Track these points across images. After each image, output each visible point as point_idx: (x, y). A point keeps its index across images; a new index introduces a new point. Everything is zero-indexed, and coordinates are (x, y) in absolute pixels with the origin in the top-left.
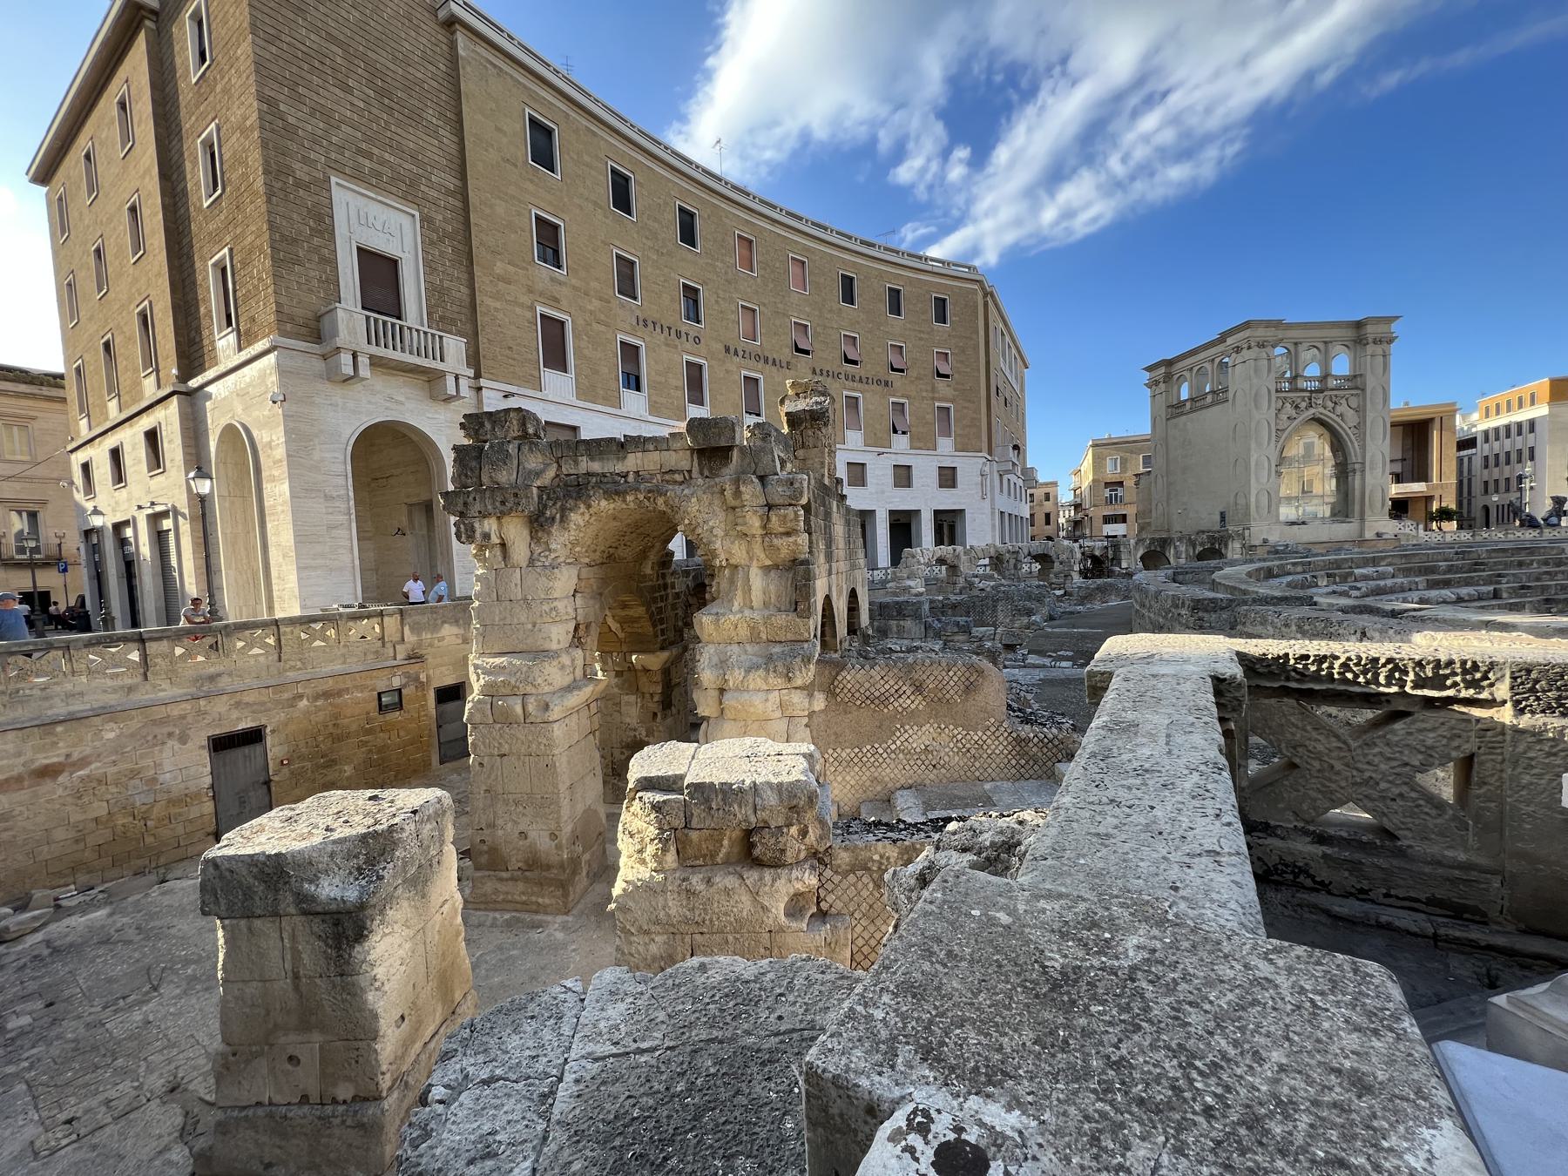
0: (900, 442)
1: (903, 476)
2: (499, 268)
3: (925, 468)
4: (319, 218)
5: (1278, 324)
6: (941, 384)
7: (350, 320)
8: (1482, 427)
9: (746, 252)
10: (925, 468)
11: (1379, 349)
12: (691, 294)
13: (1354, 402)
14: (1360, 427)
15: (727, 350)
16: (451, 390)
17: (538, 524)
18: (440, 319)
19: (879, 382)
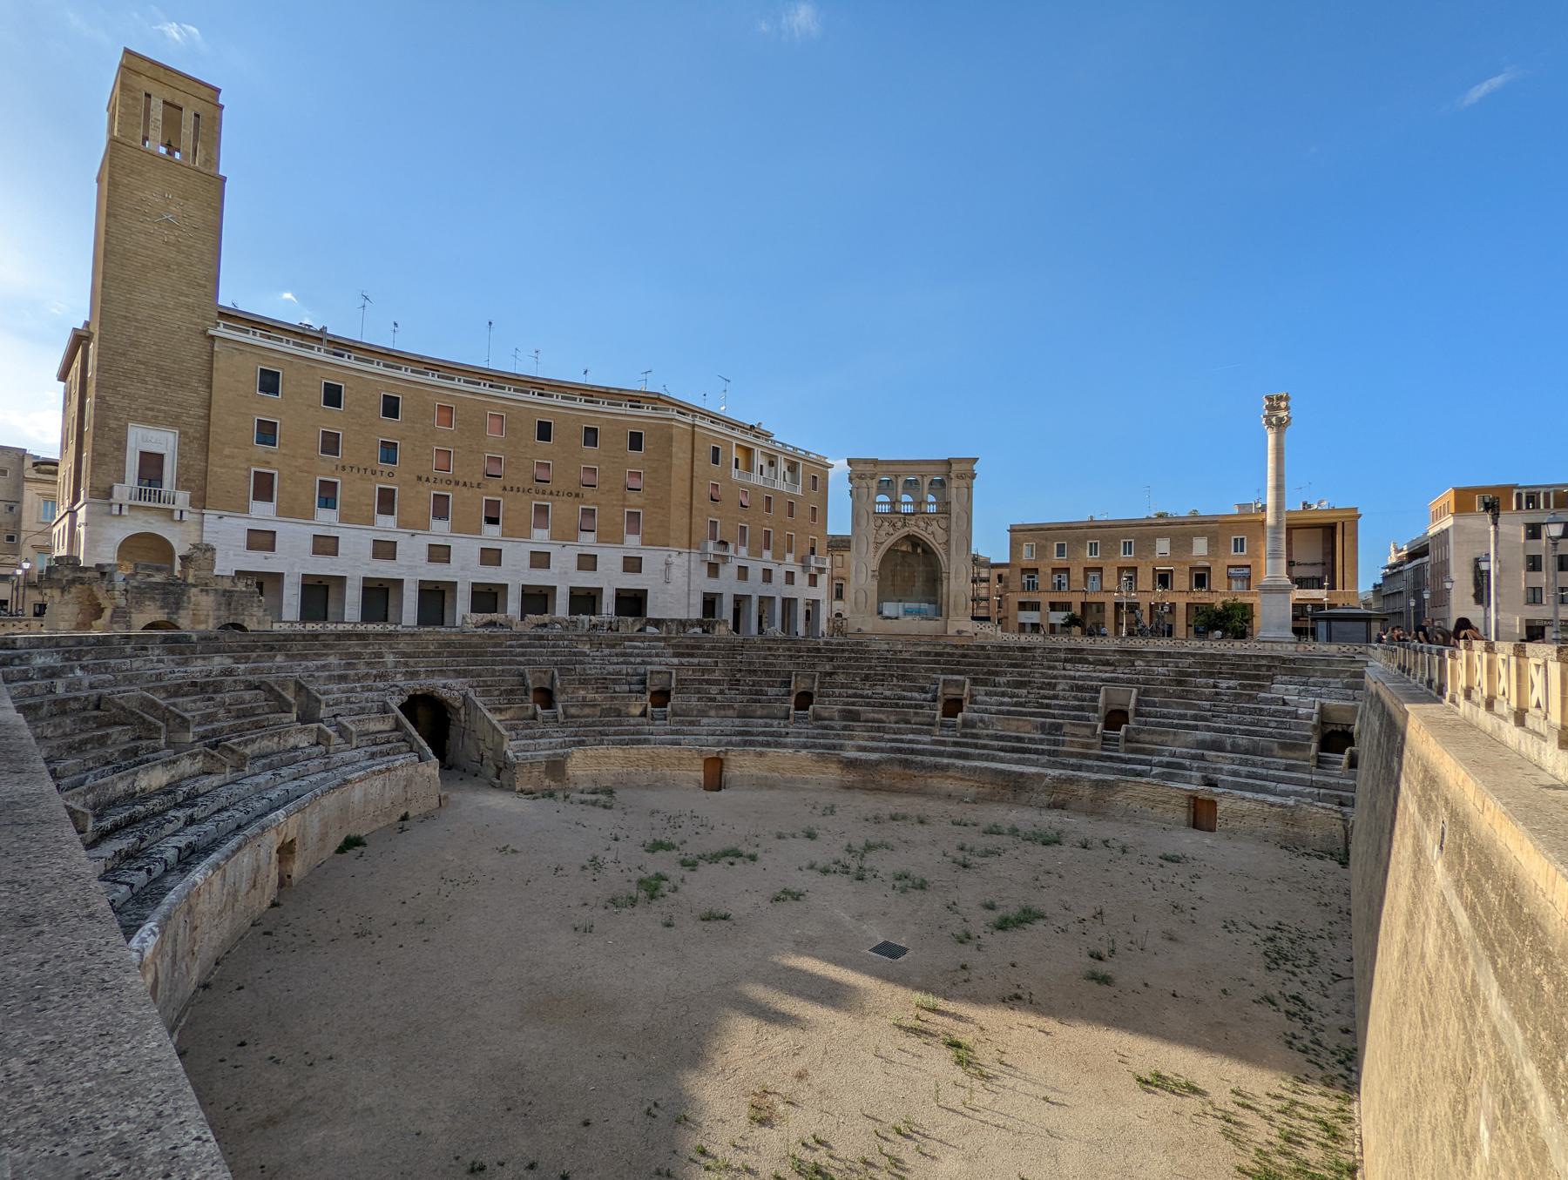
0: (588, 538)
1: (588, 562)
2: (227, 451)
3: (610, 559)
4: (119, 443)
5: (875, 462)
6: (632, 496)
7: (124, 491)
8: (1431, 533)
9: (447, 415)
10: (610, 559)
11: (963, 483)
12: (389, 451)
13: (943, 524)
14: (947, 542)
15: (419, 478)
16: (177, 515)
17: (63, 590)
18: (182, 484)
19: (570, 494)
